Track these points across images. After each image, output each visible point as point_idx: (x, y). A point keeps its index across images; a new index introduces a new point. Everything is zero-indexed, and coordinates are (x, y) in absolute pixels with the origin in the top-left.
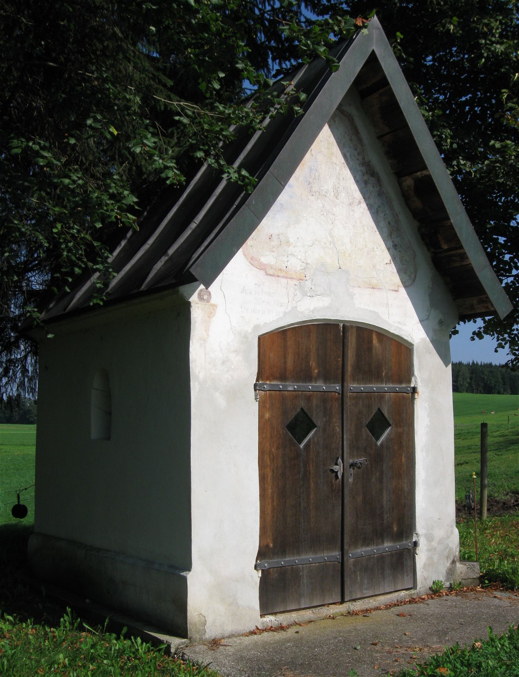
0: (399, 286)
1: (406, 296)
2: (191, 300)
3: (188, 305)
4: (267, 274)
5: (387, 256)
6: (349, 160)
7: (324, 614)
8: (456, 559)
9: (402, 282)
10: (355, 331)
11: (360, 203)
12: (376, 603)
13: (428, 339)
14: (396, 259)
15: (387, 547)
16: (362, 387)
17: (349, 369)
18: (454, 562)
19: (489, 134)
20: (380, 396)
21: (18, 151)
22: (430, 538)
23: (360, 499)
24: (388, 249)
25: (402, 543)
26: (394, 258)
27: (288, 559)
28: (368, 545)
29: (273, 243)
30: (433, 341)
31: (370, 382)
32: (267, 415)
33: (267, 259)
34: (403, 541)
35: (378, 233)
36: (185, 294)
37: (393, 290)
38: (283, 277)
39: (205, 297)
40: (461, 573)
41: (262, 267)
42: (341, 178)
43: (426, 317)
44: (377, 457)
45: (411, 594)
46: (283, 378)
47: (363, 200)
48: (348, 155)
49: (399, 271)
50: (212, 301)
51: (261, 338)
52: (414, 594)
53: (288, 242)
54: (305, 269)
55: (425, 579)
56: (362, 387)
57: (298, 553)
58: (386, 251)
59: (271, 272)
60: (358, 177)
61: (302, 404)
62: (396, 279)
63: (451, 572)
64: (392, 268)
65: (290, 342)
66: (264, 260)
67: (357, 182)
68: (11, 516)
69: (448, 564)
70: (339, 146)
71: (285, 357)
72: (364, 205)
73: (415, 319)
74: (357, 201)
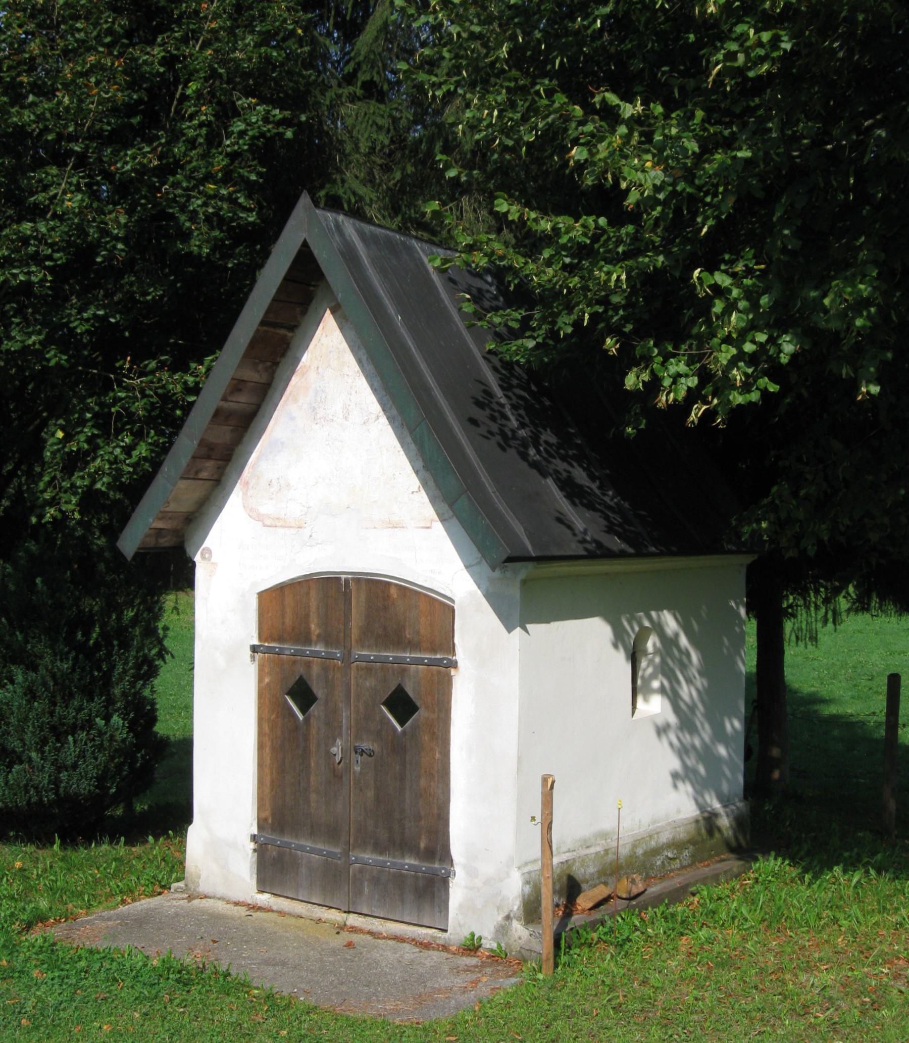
0: (432, 521)
1: (445, 533)
2: (195, 560)
3: (194, 564)
4: (265, 525)
5: (414, 482)
6: (366, 365)
7: (318, 915)
8: (512, 915)
9: (438, 514)
10: (364, 587)
11: (378, 418)
12: (384, 930)
13: (479, 592)
14: (429, 483)
15: (406, 864)
16: (371, 654)
17: (355, 633)
18: (508, 918)
19: (849, 181)
20: (402, 667)
21: (569, 330)
22: (472, 872)
23: (370, 794)
24: (417, 472)
25: (431, 865)
26: (424, 484)
27: (286, 840)
28: (381, 853)
29: (272, 490)
30: (487, 596)
31: (387, 648)
32: (267, 680)
33: (267, 508)
34: (434, 863)
35: (402, 453)
36: (192, 556)
37: (423, 528)
38: (282, 527)
39: (207, 556)
40: (520, 938)
41: (260, 518)
42: (353, 392)
43: (475, 562)
44: (398, 748)
45: (436, 937)
46: (280, 639)
47: (382, 413)
48: (364, 358)
49: (433, 501)
50: (213, 560)
51: (264, 597)
52: (440, 938)
53: (288, 485)
54: (306, 514)
55: (460, 926)
56: (371, 654)
57: (297, 837)
58: (414, 475)
59: (268, 522)
60: (376, 384)
61: (301, 670)
62: (429, 511)
63: (502, 930)
64: (423, 497)
65: (289, 600)
66: (263, 510)
67: (374, 390)
68: (888, 673)
69: (500, 918)
70: (352, 351)
71: (283, 616)
72: (384, 420)
73: (458, 564)
74: (374, 416)
